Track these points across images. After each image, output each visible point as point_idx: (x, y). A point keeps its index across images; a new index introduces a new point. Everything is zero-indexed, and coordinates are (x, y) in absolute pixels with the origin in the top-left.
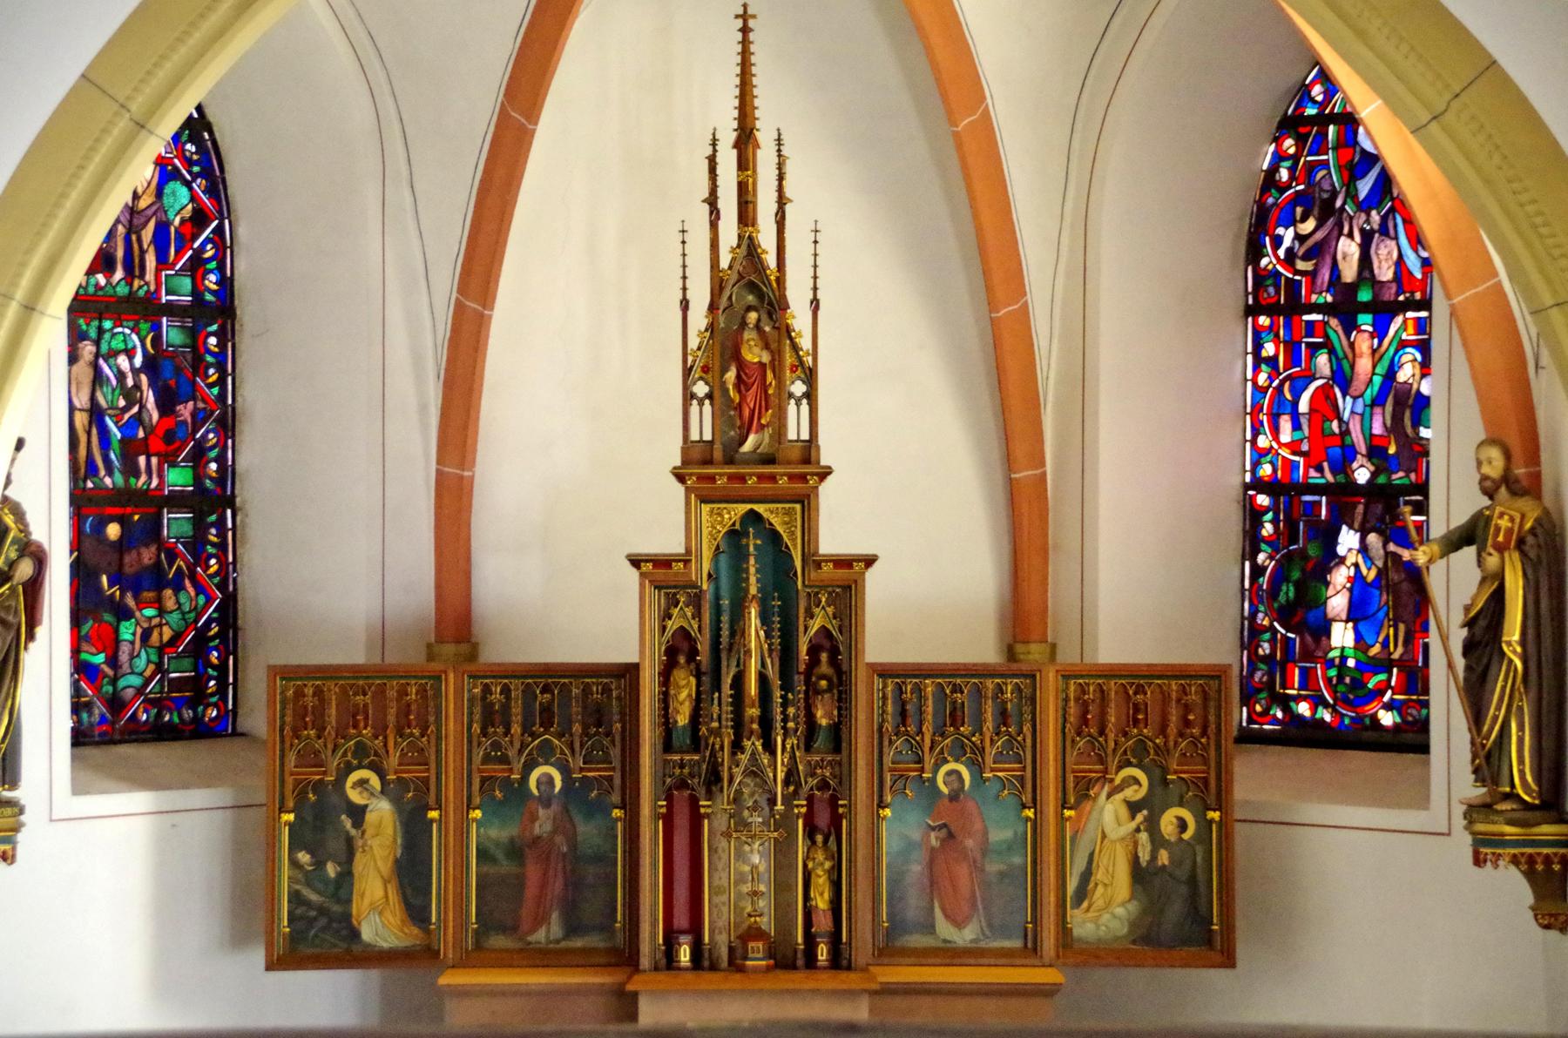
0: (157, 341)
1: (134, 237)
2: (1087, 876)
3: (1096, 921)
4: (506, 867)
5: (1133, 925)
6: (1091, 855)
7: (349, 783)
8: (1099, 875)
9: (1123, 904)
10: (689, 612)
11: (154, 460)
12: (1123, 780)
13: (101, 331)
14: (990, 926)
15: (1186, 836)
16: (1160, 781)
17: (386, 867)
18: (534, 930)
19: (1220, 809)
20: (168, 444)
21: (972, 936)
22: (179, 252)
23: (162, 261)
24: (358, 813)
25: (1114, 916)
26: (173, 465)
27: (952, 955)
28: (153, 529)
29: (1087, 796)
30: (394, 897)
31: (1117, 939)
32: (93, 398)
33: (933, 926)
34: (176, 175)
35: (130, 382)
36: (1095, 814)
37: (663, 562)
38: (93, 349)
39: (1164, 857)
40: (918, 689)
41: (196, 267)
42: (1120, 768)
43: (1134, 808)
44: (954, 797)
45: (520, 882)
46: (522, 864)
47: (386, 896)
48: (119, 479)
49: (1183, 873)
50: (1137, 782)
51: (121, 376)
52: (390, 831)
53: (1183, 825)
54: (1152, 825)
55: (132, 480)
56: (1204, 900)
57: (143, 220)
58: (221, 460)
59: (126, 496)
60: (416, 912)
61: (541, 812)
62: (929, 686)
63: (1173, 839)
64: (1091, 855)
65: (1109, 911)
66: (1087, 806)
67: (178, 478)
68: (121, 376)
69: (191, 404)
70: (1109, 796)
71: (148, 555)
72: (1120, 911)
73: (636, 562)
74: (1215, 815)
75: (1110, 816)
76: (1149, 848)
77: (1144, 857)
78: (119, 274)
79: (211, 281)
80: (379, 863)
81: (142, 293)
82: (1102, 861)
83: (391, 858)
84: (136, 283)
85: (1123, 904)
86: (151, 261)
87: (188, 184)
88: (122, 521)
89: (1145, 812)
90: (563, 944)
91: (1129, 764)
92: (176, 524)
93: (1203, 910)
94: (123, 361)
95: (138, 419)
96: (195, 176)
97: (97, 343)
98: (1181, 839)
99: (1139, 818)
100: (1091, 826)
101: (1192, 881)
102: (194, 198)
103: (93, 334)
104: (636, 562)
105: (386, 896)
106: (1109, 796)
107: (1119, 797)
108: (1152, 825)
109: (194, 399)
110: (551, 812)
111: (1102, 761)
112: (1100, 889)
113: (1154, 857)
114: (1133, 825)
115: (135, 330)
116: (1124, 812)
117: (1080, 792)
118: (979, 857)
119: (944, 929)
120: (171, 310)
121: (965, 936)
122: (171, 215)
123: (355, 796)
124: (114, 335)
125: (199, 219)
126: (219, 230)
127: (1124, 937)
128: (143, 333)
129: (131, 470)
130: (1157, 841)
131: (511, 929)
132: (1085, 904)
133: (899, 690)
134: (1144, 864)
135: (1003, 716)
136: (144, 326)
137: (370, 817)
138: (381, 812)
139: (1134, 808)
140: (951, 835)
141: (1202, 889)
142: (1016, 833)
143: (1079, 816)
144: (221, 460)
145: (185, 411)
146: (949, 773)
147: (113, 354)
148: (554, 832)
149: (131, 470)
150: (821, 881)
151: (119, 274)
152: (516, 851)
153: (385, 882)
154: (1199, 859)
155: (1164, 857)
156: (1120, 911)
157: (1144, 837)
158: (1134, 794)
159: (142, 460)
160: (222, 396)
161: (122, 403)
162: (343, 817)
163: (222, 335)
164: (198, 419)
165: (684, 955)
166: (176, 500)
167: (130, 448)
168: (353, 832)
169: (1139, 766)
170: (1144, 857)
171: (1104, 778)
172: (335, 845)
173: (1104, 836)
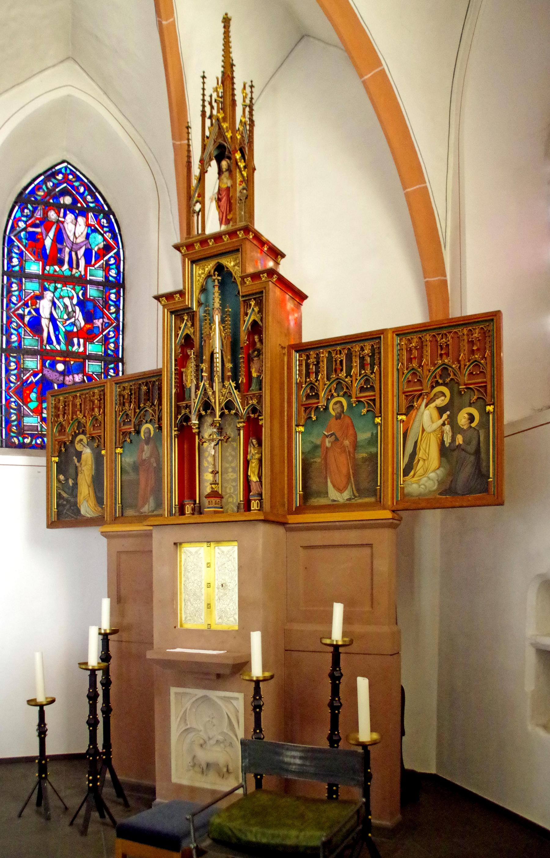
0: (84, 294)
1: (73, 254)
2: (413, 454)
3: (418, 482)
4: (132, 476)
5: (441, 483)
6: (416, 443)
7: (76, 442)
8: (421, 454)
9: (434, 471)
10: (189, 324)
11: (82, 341)
13: (56, 288)
14: (358, 490)
15: (473, 425)
16: (456, 394)
17: (89, 479)
18: (143, 506)
19: (493, 404)
20: (89, 335)
21: (348, 497)
22: (97, 260)
23: (88, 263)
24: (79, 455)
25: (429, 478)
26: (92, 342)
27: (334, 507)
28: (81, 369)
29: (412, 406)
30: (92, 494)
31: (430, 492)
32: (51, 314)
33: (327, 493)
34: (95, 230)
35: (70, 309)
36: (418, 418)
37: (169, 296)
38: (52, 295)
39: (460, 439)
41: (107, 268)
42: (433, 387)
43: (441, 411)
44: (338, 417)
45: (137, 483)
46: (138, 474)
47: (89, 493)
48: (63, 347)
49: (472, 448)
51: (66, 307)
52: (90, 463)
53: (471, 418)
55: (70, 348)
56: (484, 464)
57: (78, 247)
58: (116, 344)
59: (67, 354)
60: (100, 501)
61: (146, 447)
62: (324, 355)
63: (465, 427)
64: (416, 443)
65: (428, 475)
66: (413, 413)
67: (95, 348)
68: (66, 307)
69: (101, 320)
70: (426, 405)
71: (78, 378)
72: (432, 475)
73: (158, 298)
74: (490, 408)
76: (450, 434)
77: (447, 440)
78: (66, 266)
79: (113, 273)
80: (87, 478)
81: (77, 275)
82: (422, 446)
83: (91, 475)
84: (74, 271)
85: (434, 471)
86: (82, 262)
87: (103, 235)
88: (64, 363)
89: (448, 413)
90: (155, 513)
91: (438, 384)
92: (93, 367)
94: (67, 301)
95: (74, 324)
96: (105, 232)
97: (54, 293)
98: (471, 427)
99: (445, 416)
100: (416, 424)
101: (477, 452)
102: (105, 239)
103: (52, 289)
104: (158, 298)
105: (89, 493)
106: (426, 405)
107: (433, 405)
108: (452, 421)
109: (103, 318)
110: (149, 446)
112: (421, 463)
113: (453, 439)
114: (441, 422)
115: (74, 289)
116: (435, 414)
118: (351, 450)
119: (333, 494)
120: (92, 283)
121: (343, 497)
122: (93, 246)
123: (79, 447)
124: (62, 290)
125: (107, 248)
126: (117, 254)
128: (77, 290)
129: (69, 343)
130: (456, 429)
131: (134, 506)
132: (412, 473)
134: (447, 445)
136: (78, 288)
137: (83, 457)
138: (87, 453)
139: (441, 411)
140: (337, 439)
141: (483, 455)
142: (372, 433)
143: (408, 421)
144: (116, 344)
145: (98, 323)
146: (336, 403)
147: (61, 297)
148: (151, 456)
149: (69, 343)
150: (253, 465)
151: (66, 266)
152: (136, 468)
153: (89, 487)
154: (482, 439)
155: (460, 439)
156: (432, 475)
157: (447, 428)
158: (440, 402)
159: (75, 340)
160: (117, 319)
161: (66, 317)
162: (74, 458)
163: (118, 294)
164: (106, 326)
166: (91, 357)
167: (69, 336)
168: (78, 464)
169: (445, 384)
170: (447, 440)
172: (71, 471)
173: (423, 430)
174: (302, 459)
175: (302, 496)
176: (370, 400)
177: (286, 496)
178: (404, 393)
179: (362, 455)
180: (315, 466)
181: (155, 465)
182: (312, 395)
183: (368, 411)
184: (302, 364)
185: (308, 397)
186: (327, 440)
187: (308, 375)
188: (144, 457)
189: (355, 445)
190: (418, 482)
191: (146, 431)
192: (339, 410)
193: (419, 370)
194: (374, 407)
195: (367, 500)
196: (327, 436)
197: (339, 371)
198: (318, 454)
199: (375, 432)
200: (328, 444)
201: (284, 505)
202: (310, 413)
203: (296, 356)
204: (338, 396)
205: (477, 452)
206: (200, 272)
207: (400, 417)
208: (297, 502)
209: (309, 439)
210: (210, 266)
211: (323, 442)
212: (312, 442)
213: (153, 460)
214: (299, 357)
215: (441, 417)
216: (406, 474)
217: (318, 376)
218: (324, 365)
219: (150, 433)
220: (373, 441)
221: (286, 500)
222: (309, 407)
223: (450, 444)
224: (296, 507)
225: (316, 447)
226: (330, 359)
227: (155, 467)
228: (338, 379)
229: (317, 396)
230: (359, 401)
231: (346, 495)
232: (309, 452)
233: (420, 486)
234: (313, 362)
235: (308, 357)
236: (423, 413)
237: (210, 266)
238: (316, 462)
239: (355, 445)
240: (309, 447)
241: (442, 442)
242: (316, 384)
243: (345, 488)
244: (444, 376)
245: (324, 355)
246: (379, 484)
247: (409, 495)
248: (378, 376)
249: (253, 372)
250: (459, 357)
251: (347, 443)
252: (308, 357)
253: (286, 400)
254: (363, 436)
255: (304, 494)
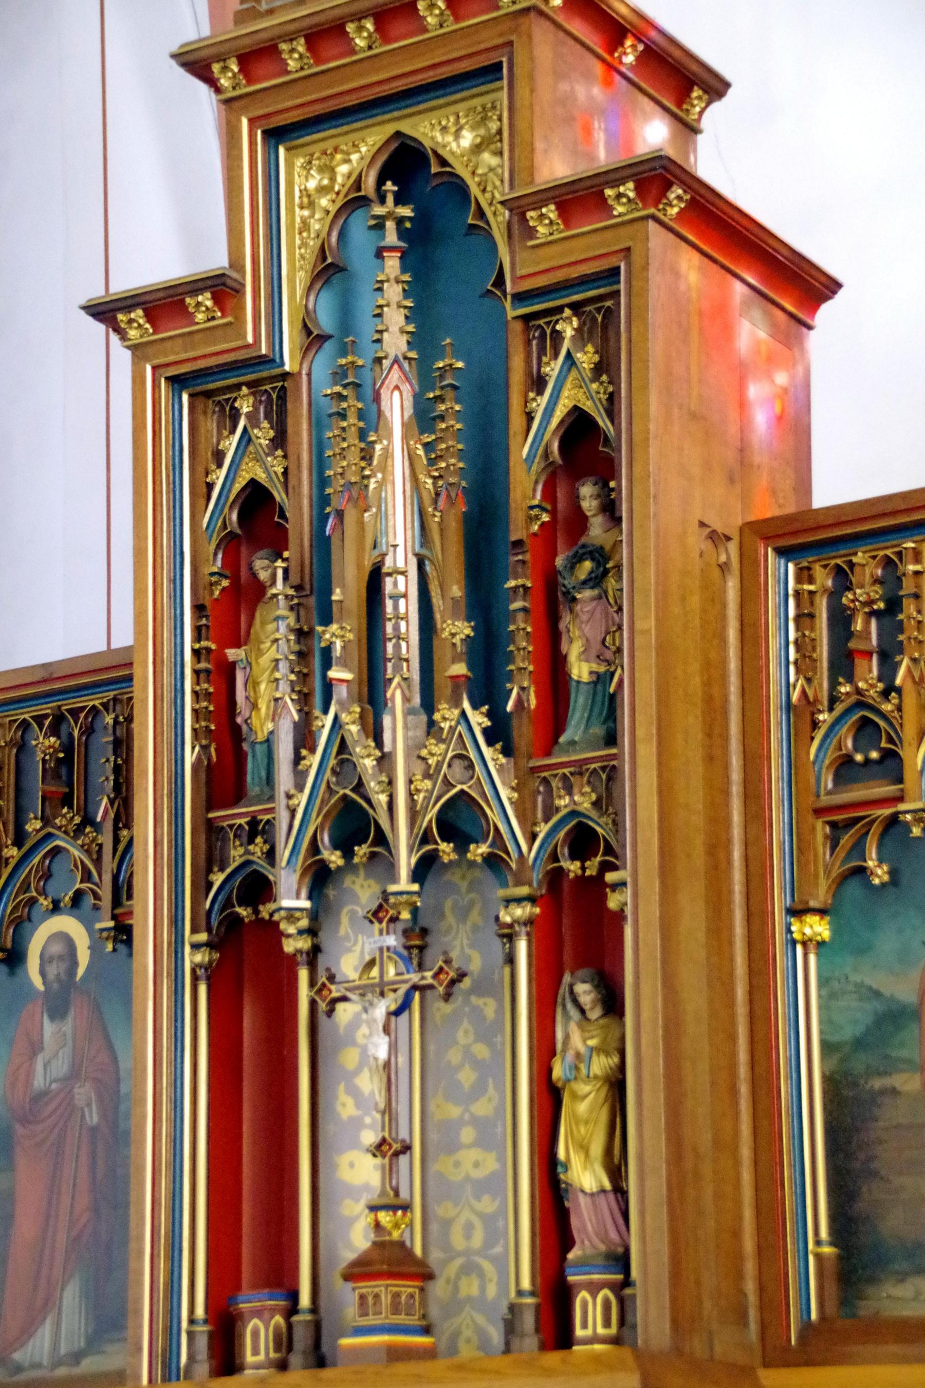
10: (263, 435)
37: (163, 305)
61: (49, 1028)
73: (105, 312)
104: (105, 312)
148: (74, 1074)
150: (582, 1108)
165: (258, 1338)
174: (827, 1080)
175: (831, 1268)
177: (750, 1267)
180: (891, 1115)
181: (93, 1117)
182: (867, 761)
184: (811, 616)
185: (845, 769)
187: (843, 663)
188: (39, 1082)
191: (57, 948)
198: (904, 1053)
201: (742, 1318)
202: (858, 849)
203: (781, 574)
206: (315, 181)
208: (809, 1297)
209: (855, 978)
210: (357, 153)
212: (877, 994)
213: (83, 1093)
214: (799, 580)
217: (896, 667)
219: (74, 964)
221: (750, 1287)
224: (807, 1328)
225: (892, 1018)
227: (94, 1130)
232: (859, 1044)
234: (870, 602)
235: (843, 578)
237: (357, 153)
238: (894, 1092)
240: (855, 1019)
242: (887, 707)
249: (573, 657)
253: (736, 789)
255: (840, 1258)
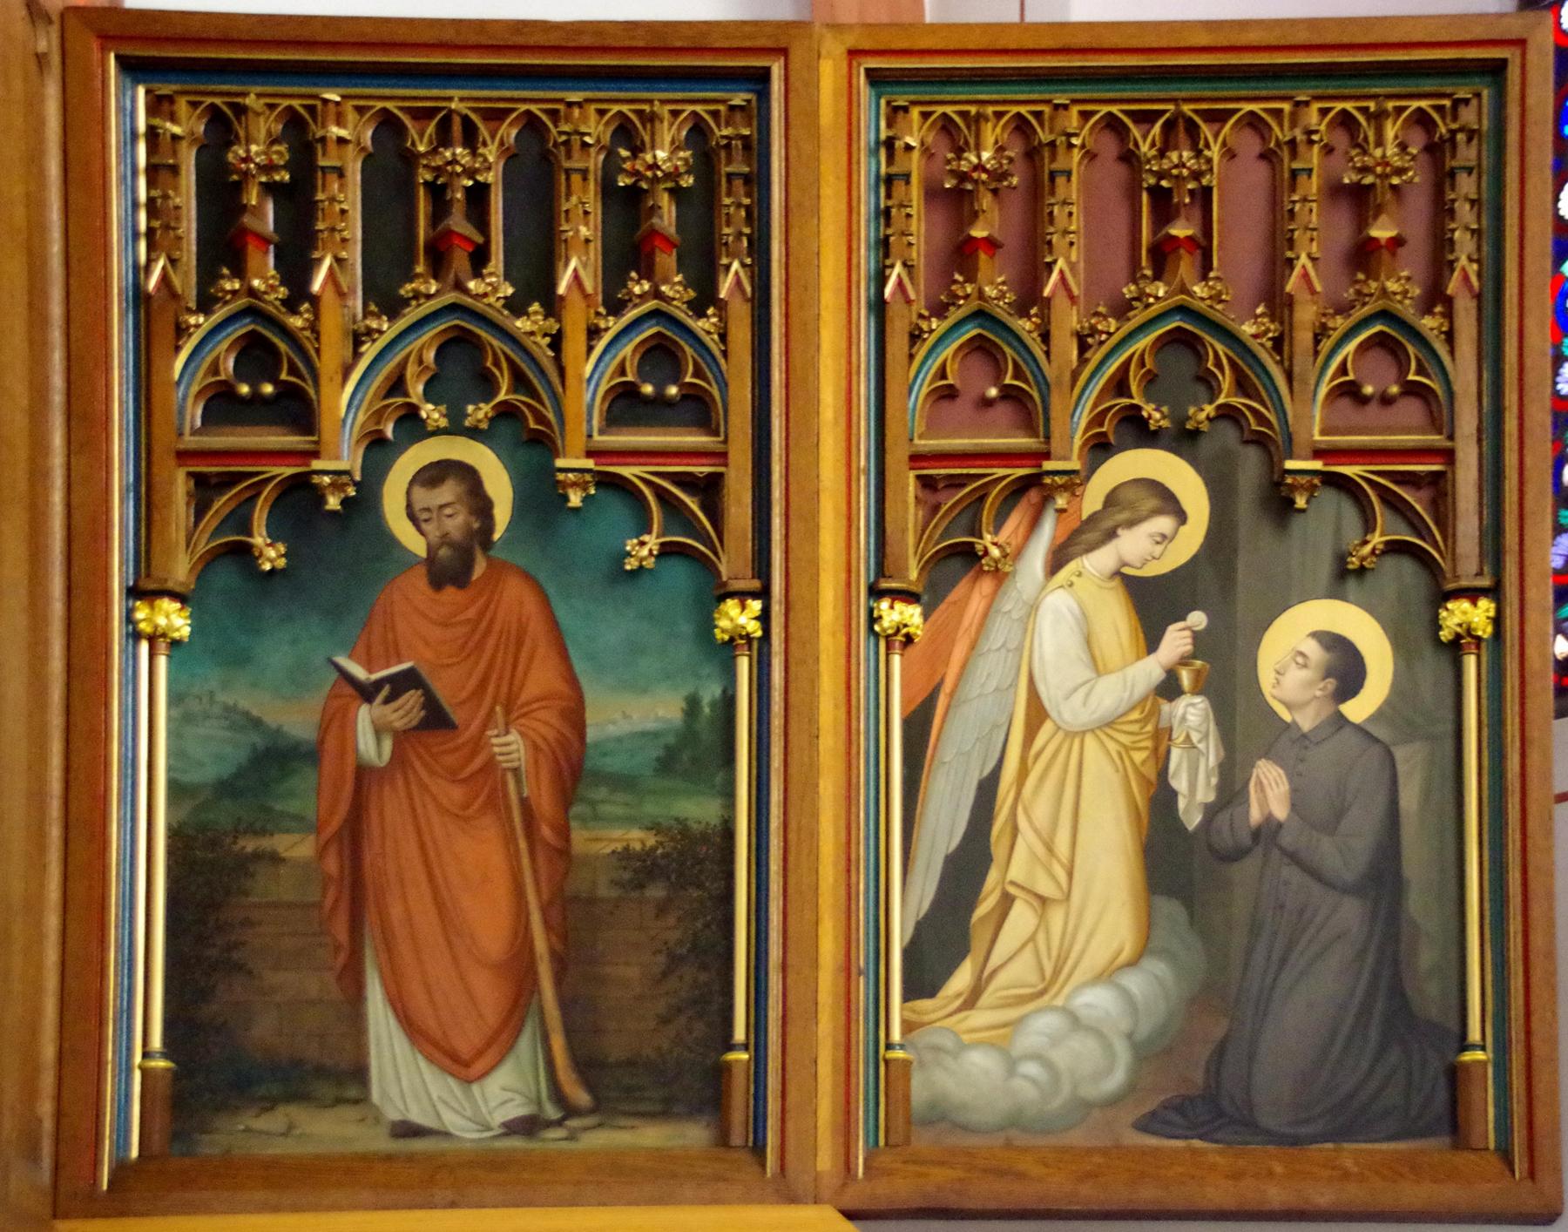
2: (969, 865)
3: (1001, 1041)
5: (1151, 1053)
6: (987, 790)
8: (1018, 864)
9: (1107, 976)
12: (1111, 500)
14: (588, 1066)
15: (1358, 709)
19: (1495, 592)
21: (517, 1110)
25: (1075, 1021)
29: (968, 556)
31: (1084, 1107)
33: (359, 1073)
36: (1001, 632)
39: (1271, 792)
40: (299, 134)
42: (1100, 449)
43: (1153, 603)
44: (449, 570)
49: (1346, 853)
50: (1169, 503)
53: (1346, 668)
54: (1224, 671)
56: (1427, 957)
62: (347, 133)
63: (1306, 721)
64: (987, 790)
66: (973, 596)
70: (1057, 561)
72: (1098, 1001)
75: (1060, 635)
76: (1212, 754)
77: (1194, 789)
82: (1030, 811)
85: (1107, 976)
89: (1198, 619)
91: (1138, 431)
93: (1429, 996)
98: (1341, 721)
99: (1176, 640)
100: (990, 671)
106: (1057, 561)
107: (1099, 561)
108: (1224, 671)
111: (1024, 406)
112: (1021, 918)
113: (1231, 789)
114: (1151, 669)
116: (1115, 618)
117: (954, 533)
118: (545, 803)
119: (402, 1079)
127: (1113, 1102)
132: (961, 979)
133: (223, 128)
134: (1192, 819)
135: (628, 252)
139: (1153, 603)
140: (435, 718)
141: (1419, 903)
142: (693, 704)
143: (941, 642)
146: (434, 474)
155: (1271, 792)
156: (1098, 1001)
157: (1191, 712)
158: (1159, 547)
169: (1183, 440)
170: (1194, 789)
171: (1033, 488)
173: (1037, 713)
174: (173, 834)
175: (162, 1088)
176: (682, 480)
178: (917, 459)
179: (613, 834)
180: (267, 887)
182: (256, 396)
183: (667, 551)
184: (174, 170)
185: (222, 405)
186: (364, 716)
189: (572, 768)
190: (1001, 1041)
192: (457, 523)
193: (1024, 326)
194: (708, 531)
195: (651, 1136)
196: (367, 692)
197: (460, 261)
198: (293, 806)
199: (711, 692)
200: (370, 746)
202: (240, 520)
204: (456, 428)
205: (1383, 878)
207: (893, 614)
208: (126, 1126)
211: (336, 721)
212: (257, 723)
215: (1152, 644)
216: (921, 984)
218: (345, 201)
220: (701, 750)
222: (232, 480)
223: (1211, 811)
224: (122, 1169)
225: (275, 760)
226: (390, 170)
228: (453, 308)
229: (297, 409)
230: (609, 482)
231: (505, 1092)
232: (227, 788)
233: (1011, 1065)
234: (269, 168)
236: (1033, 608)
238: (275, 859)
239: (572, 768)
240: (219, 755)
241: (1162, 799)
243: (500, 1042)
244: (1190, 386)
245: (347, 133)
246: (739, 1034)
247: (940, 1116)
248: (741, 335)
250: (1284, 279)
251: (511, 746)
252: (223, 128)
254: (632, 712)
255: (176, 1076)
